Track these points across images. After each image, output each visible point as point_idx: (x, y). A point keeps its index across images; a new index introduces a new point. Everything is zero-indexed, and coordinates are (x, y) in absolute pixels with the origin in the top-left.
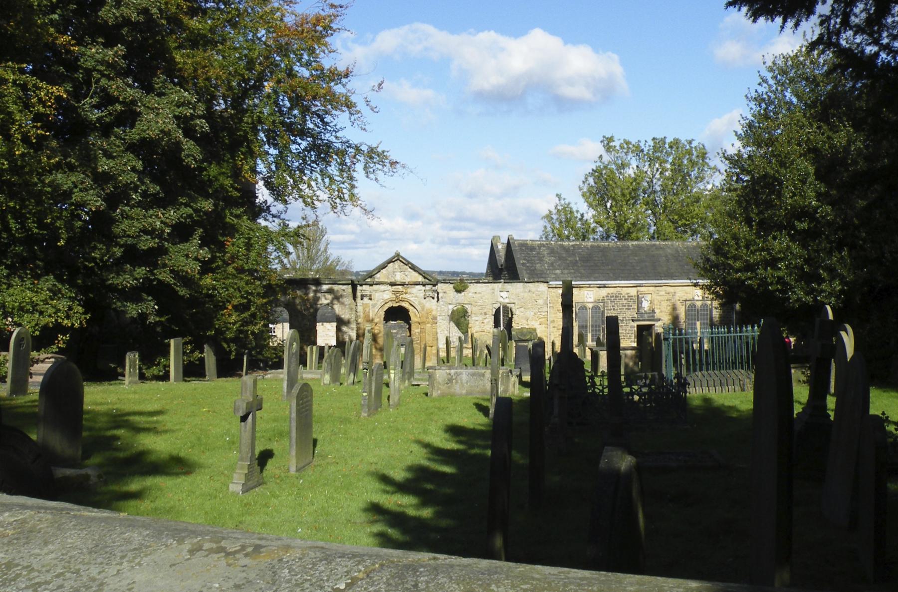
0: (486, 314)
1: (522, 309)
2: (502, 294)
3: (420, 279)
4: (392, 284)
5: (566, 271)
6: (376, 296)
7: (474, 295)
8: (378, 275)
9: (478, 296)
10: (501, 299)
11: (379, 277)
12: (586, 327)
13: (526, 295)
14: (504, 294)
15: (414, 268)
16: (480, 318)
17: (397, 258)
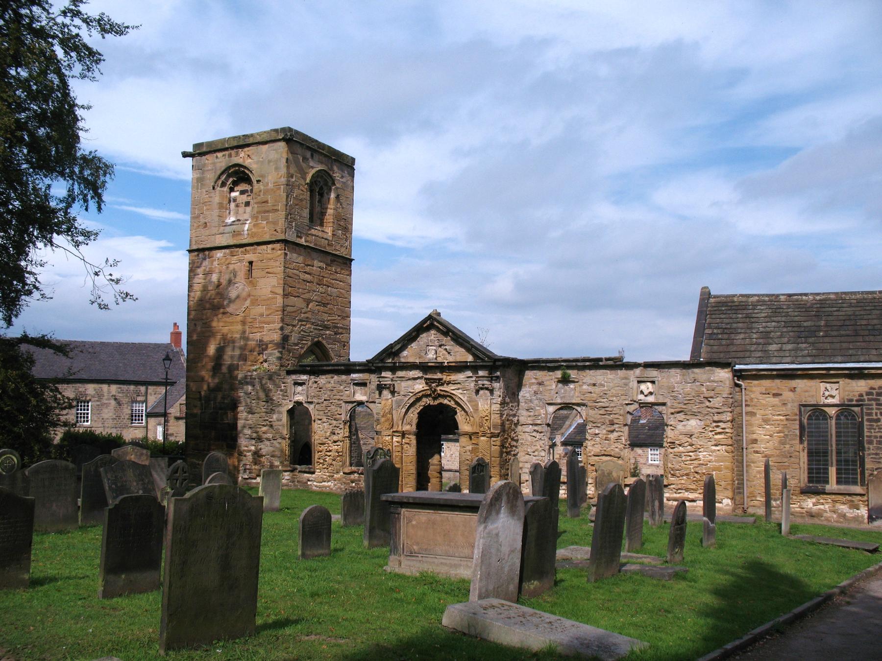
0: (612, 423)
1: (681, 416)
2: (643, 387)
3: (470, 358)
4: (424, 367)
5: (790, 347)
6: (403, 387)
7: (591, 389)
8: (405, 353)
9: (596, 389)
10: (641, 397)
11: (408, 355)
12: (826, 453)
13: (688, 388)
14: (646, 387)
15: (460, 339)
16: (602, 431)
17: (430, 323)
